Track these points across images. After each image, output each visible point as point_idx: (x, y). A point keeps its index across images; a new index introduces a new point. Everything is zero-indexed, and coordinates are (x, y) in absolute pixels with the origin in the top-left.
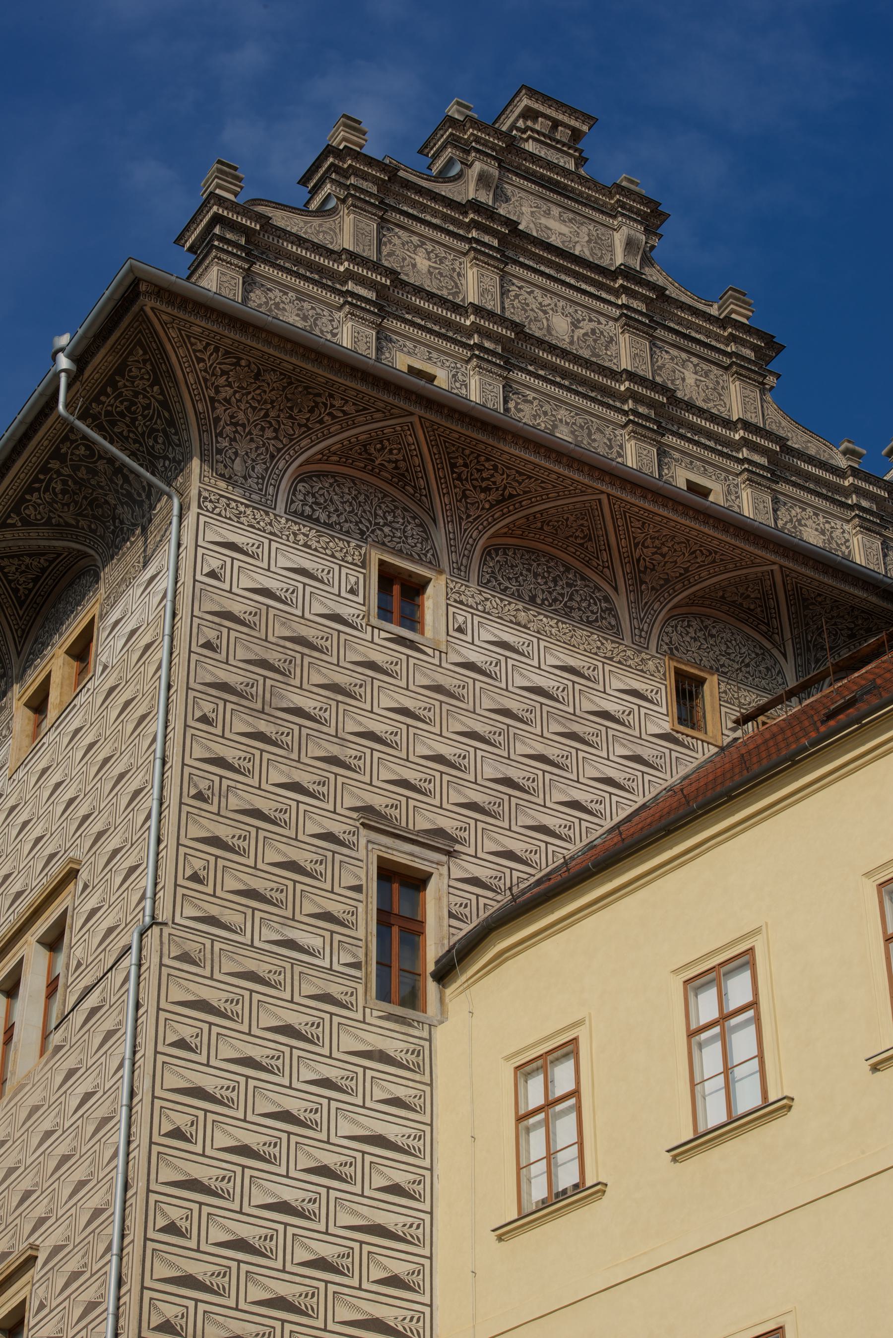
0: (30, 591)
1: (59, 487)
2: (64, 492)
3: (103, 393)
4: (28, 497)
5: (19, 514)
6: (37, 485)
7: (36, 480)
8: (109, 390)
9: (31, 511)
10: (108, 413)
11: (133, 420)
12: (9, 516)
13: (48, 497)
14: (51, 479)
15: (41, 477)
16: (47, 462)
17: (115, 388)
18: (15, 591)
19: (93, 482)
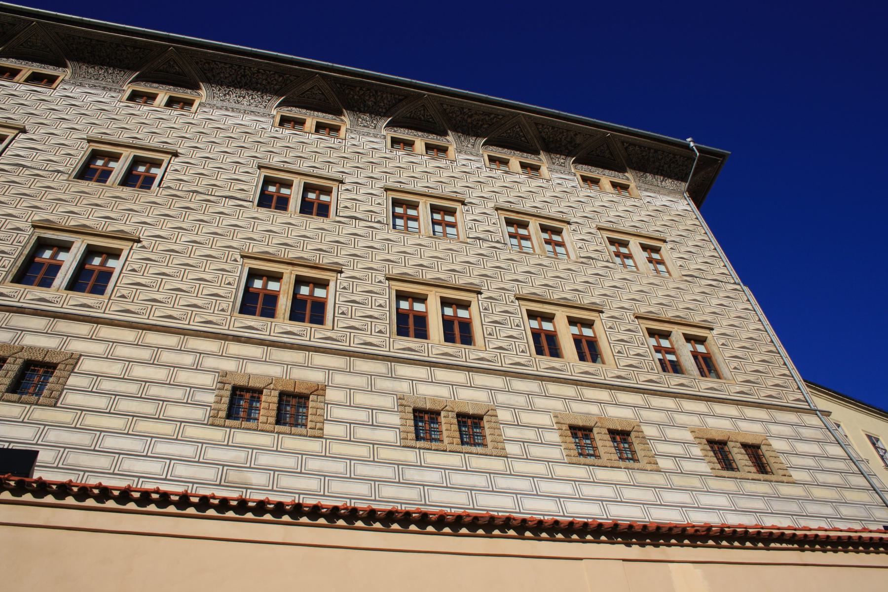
0: (593, 155)
1: (644, 154)
2: (643, 156)
3: (684, 157)
4: (637, 146)
5: (629, 146)
6: (642, 148)
7: (645, 148)
8: (685, 159)
9: (631, 149)
10: (677, 161)
11: (677, 168)
12: (627, 143)
13: (639, 152)
14: (646, 151)
15: (646, 148)
16: (652, 149)
17: (686, 160)
18: (593, 151)
19: (650, 163)
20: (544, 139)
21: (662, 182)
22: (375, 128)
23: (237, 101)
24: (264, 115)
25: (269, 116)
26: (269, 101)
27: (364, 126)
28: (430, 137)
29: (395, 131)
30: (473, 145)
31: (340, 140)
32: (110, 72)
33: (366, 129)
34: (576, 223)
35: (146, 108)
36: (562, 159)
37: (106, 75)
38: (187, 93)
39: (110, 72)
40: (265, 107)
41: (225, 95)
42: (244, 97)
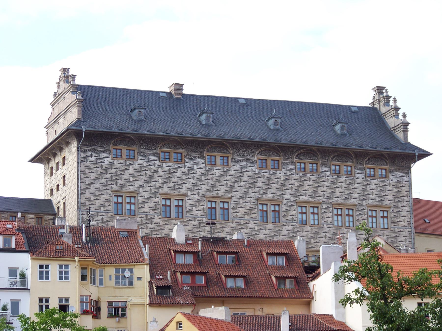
20: (355, 154)
21: (401, 163)
22: (291, 159)
23: (243, 154)
24: (253, 162)
25: (255, 161)
26: (254, 152)
27: (288, 159)
28: (311, 158)
29: (299, 158)
30: (327, 160)
31: (280, 171)
32: (198, 147)
33: (288, 160)
34: (359, 204)
35: (215, 169)
36: (362, 159)
37: (197, 149)
38: (225, 153)
39: (198, 147)
40: (253, 155)
41: (238, 152)
42: (245, 152)
